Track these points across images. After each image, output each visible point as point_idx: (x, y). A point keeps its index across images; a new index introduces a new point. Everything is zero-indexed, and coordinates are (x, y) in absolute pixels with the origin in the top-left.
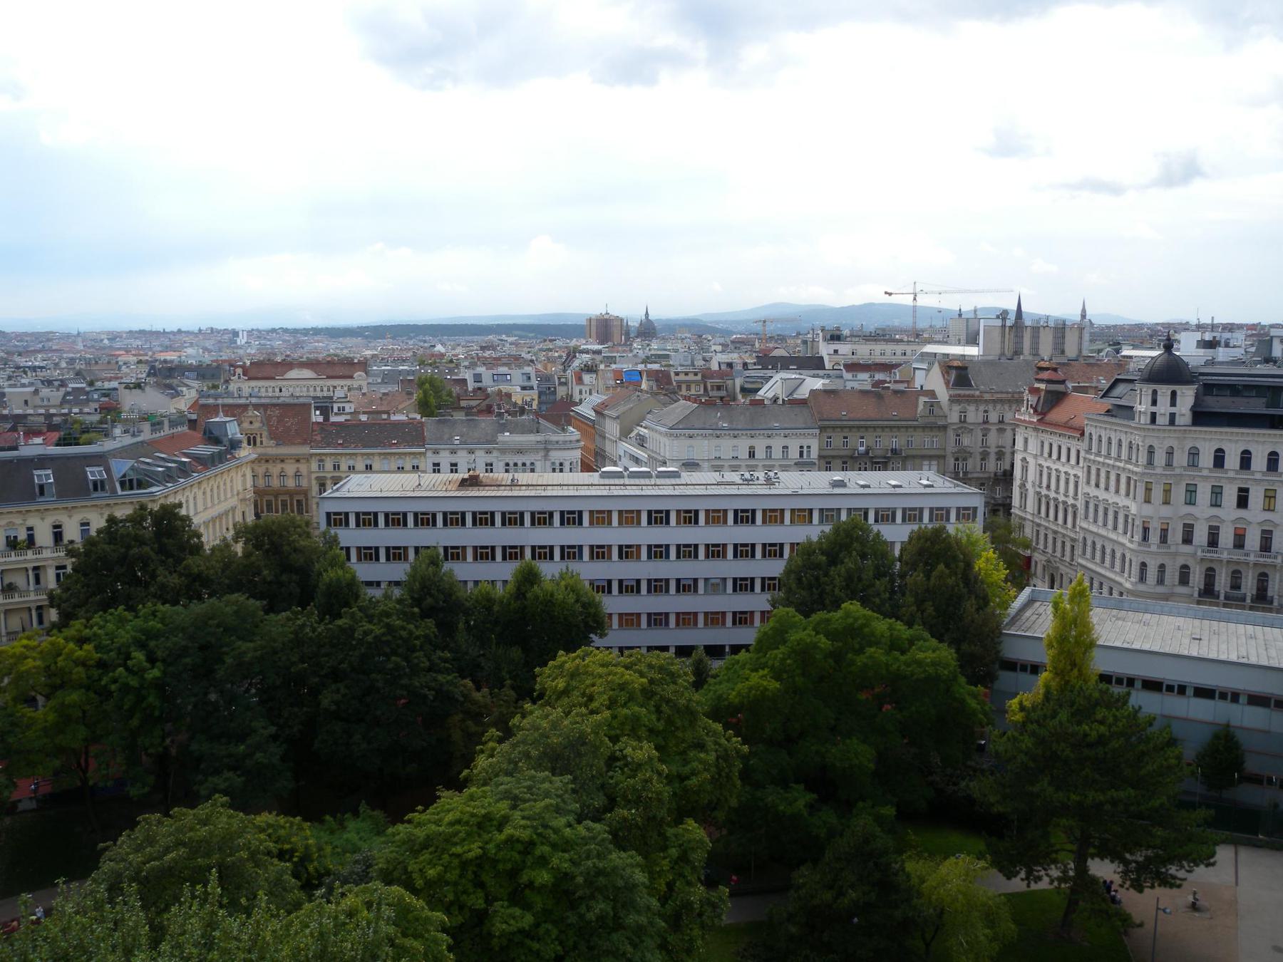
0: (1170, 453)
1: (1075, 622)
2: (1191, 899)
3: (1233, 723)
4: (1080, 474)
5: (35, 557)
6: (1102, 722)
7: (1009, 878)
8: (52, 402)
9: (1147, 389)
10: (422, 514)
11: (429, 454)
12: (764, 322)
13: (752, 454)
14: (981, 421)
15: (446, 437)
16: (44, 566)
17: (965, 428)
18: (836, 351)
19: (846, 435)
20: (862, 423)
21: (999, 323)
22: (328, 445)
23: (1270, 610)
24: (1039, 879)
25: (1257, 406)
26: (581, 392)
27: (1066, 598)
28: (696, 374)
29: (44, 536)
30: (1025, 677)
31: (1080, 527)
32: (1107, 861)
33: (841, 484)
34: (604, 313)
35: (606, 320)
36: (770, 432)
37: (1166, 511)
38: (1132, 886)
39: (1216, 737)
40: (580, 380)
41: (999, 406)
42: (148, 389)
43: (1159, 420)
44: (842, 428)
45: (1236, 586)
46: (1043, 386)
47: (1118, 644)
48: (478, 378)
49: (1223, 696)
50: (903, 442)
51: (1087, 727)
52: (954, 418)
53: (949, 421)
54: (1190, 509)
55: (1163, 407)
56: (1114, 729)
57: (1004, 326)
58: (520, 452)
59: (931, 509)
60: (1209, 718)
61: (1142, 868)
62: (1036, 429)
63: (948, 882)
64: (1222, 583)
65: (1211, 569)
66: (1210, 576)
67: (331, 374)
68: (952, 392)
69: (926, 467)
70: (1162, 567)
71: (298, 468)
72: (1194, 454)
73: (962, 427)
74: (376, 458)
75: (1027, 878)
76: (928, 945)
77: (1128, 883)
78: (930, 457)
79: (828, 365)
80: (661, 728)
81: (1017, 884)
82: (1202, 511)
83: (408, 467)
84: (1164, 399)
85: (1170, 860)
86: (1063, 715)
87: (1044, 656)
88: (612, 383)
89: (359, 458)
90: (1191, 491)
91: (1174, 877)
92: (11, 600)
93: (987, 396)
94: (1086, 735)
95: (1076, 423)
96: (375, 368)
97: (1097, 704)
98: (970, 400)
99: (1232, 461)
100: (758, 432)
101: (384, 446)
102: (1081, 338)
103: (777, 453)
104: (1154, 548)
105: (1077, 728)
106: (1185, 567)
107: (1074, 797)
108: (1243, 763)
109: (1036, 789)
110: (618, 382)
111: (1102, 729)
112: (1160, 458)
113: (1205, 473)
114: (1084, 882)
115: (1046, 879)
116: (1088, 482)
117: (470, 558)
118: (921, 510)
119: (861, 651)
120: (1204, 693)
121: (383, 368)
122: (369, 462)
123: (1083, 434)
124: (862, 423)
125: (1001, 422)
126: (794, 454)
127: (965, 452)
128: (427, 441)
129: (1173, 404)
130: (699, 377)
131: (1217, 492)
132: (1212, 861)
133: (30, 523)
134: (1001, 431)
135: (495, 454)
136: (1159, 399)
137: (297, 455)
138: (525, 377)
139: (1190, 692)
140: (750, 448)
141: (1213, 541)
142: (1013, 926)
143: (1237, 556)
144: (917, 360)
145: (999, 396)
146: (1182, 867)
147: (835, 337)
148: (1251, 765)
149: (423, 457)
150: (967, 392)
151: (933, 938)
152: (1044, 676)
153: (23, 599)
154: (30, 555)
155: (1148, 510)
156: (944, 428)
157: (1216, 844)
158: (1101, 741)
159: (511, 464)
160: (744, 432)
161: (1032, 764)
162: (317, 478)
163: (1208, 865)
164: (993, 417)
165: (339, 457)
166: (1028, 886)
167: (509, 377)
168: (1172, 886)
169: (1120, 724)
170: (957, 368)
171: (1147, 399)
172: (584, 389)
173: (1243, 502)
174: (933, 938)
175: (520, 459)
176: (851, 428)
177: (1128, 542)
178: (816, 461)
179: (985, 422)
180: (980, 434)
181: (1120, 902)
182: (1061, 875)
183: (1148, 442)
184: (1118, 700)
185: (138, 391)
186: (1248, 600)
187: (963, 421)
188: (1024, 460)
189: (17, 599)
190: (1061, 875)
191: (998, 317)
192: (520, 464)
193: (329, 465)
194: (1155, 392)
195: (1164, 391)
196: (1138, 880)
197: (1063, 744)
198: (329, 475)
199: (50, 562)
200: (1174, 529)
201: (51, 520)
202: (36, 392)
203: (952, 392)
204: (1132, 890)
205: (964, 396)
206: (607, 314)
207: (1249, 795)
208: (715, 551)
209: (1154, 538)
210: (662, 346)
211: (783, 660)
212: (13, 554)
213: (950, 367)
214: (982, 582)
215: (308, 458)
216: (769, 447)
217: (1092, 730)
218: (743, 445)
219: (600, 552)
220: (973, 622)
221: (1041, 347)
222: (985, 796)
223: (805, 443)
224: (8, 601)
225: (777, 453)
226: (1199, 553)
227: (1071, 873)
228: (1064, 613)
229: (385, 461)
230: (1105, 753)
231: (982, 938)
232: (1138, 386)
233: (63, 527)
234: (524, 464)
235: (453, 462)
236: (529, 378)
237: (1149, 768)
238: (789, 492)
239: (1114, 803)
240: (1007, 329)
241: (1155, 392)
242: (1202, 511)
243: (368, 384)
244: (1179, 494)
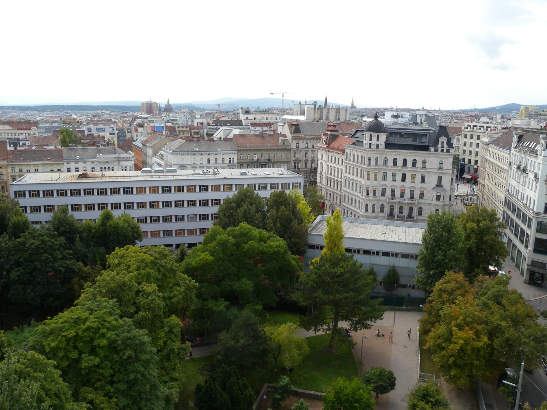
0: (377, 160)
1: (335, 228)
2: (377, 332)
3: (395, 265)
4: (343, 169)
6: (342, 267)
7: (308, 331)
9: (368, 134)
10: (60, 190)
11: (65, 164)
12: (219, 105)
13: (209, 162)
15: (73, 156)
17: (298, 150)
18: (247, 118)
19: (248, 153)
20: (256, 148)
21: (313, 106)
22: (16, 161)
23: (413, 221)
24: (319, 330)
25: (409, 141)
26: (137, 136)
27: (332, 218)
28: (187, 128)
30: (317, 251)
31: (343, 190)
32: (344, 321)
33: (245, 174)
36: (216, 152)
37: (375, 183)
38: (354, 330)
39: (390, 271)
40: (136, 131)
41: (312, 141)
43: (373, 147)
44: (247, 150)
45: (401, 212)
46: (329, 133)
47: (354, 236)
48: (89, 130)
49: (393, 255)
50: (273, 156)
51: (336, 270)
54: (384, 182)
55: (374, 142)
56: (346, 269)
57: (315, 108)
58: (107, 162)
59: (282, 184)
60: (388, 264)
61: (357, 322)
62: (326, 151)
63: (281, 334)
64: (396, 211)
65: (392, 206)
66: (392, 209)
67: (19, 128)
68: (292, 135)
69: (282, 166)
70: (374, 205)
72: (386, 160)
74: (40, 166)
75: (315, 330)
76: (276, 359)
77: (352, 328)
78: (284, 162)
79: (244, 124)
80: (160, 278)
81: (311, 333)
82: (389, 183)
83: (55, 170)
84: (374, 138)
85: (367, 319)
86: (327, 265)
87: (323, 242)
88: (150, 131)
89: (32, 166)
90: (385, 175)
91: (369, 325)
93: (307, 137)
94: (336, 273)
95: (341, 148)
96: (41, 125)
97: (340, 260)
98: (300, 138)
99: (400, 163)
100: (211, 152)
101: (44, 161)
102: (346, 113)
103: (220, 161)
104: (371, 198)
105: (332, 270)
106: (382, 205)
107: (331, 297)
108: (399, 280)
109: (316, 295)
111: (342, 270)
112: (373, 162)
113: (390, 168)
114: (336, 331)
115: (322, 330)
116: (346, 172)
117: (83, 209)
118: (278, 184)
119: (247, 243)
120: (386, 254)
121: (46, 125)
122: (36, 168)
123: (344, 152)
124: (256, 148)
125: (313, 147)
126: (227, 161)
128: (64, 158)
129: (378, 140)
130: (188, 129)
131: (394, 175)
132: (382, 317)
135: (96, 163)
136: (372, 138)
139: (381, 254)
141: (393, 195)
142: (308, 349)
143: (402, 200)
144: (280, 122)
145: (312, 137)
146: (372, 321)
147: (247, 112)
148: (402, 281)
150: (299, 135)
151: (278, 356)
152: (324, 250)
155: (368, 183)
156: (290, 150)
157: (384, 311)
158: (342, 274)
159: (103, 168)
160: (206, 152)
161: (315, 285)
162: (11, 176)
163: (380, 319)
164: (310, 146)
166: (315, 333)
168: (368, 328)
169: (349, 268)
170: (295, 125)
171: (368, 138)
172: (138, 134)
173: (404, 179)
174: (278, 356)
175: (107, 166)
176: (250, 150)
177: (361, 196)
178: (236, 164)
179: (307, 148)
181: (351, 336)
182: (327, 328)
183: (368, 155)
184: (348, 258)
186: (405, 218)
187: (297, 147)
188: (321, 163)
190: (327, 328)
191: (312, 104)
192: (107, 168)
193: (17, 170)
194: (371, 135)
195: (374, 135)
196: (356, 327)
197: (327, 277)
198: (17, 174)
200: (378, 191)
203: (292, 135)
204: (353, 331)
205: (298, 137)
206: (151, 101)
207: (402, 292)
208: (192, 203)
209: (371, 194)
210: (174, 115)
211: (214, 247)
214: (300, 213)
215: (6, 167)
216: (216, 159)
217: (338, 270)
218: (205, 158)
219: (141, 205)
220: (296, 229)
222: (298, 299)
223: (231, 157)
225: (220, 161)
226: (388, 200)
227: (331, 327)
228: (331, 224)
229: (45, 167)
230: (343, 279)
231: (295, 355)
232: (364, 133)
234: (109, 168)
235: (77, 167)
236: (113, 130)
237: (360, 284)
238: (222, 177)
239: (346, 298)
240: (316, 109)
241: (371, 135)
242: (389, 183)
243: (38, 132)
244: (380, 176)
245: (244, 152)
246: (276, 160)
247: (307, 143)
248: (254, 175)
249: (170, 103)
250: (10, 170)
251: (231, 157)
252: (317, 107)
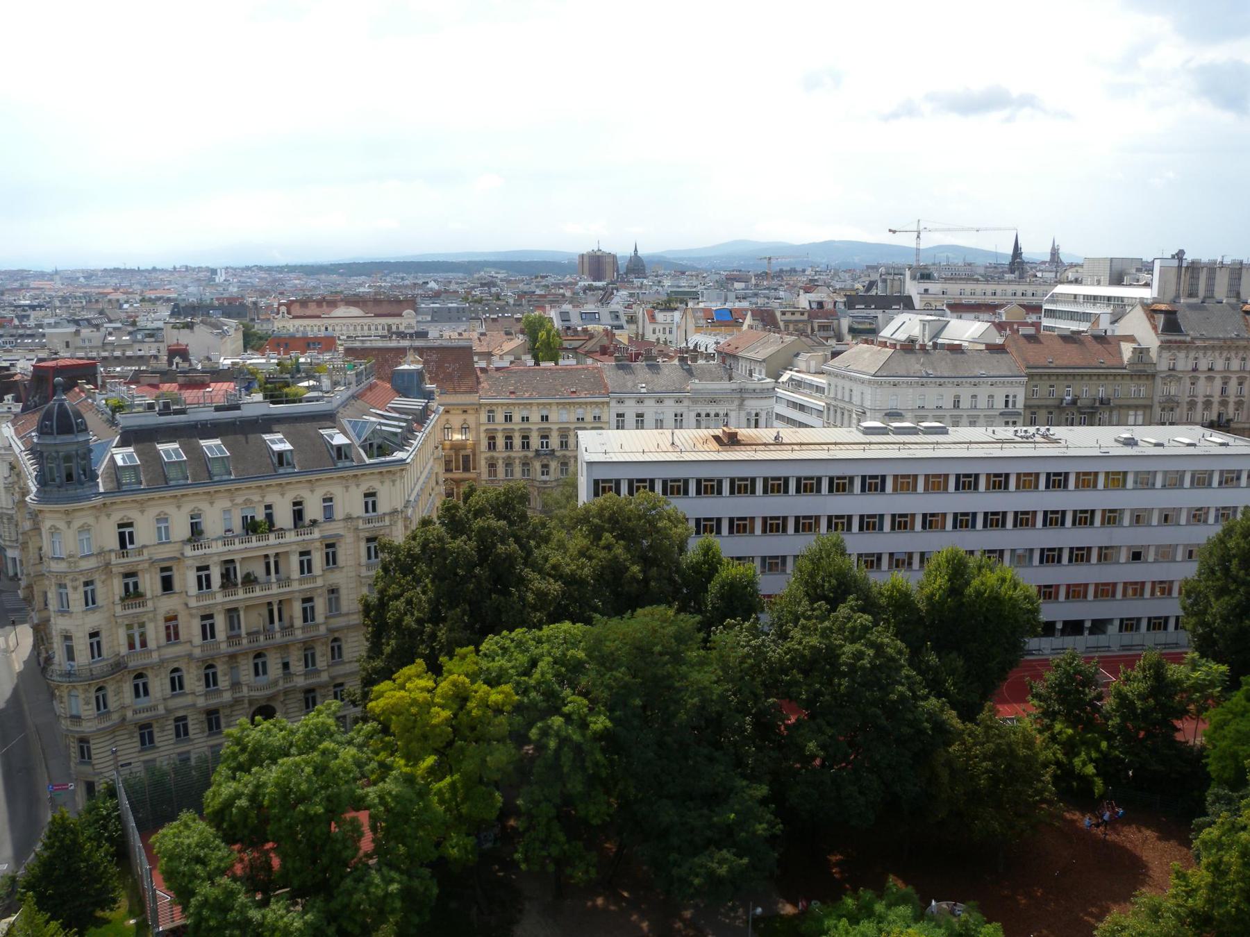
5: (278, 541)
8: (94, 343)
10: (706, 480)
11: (613, 403)
12: (770, 259)
13: (957, 404)
14: (1190, 368)
16: (287, 553)
17: (1175, 376)
18: (926, 291)
19: (1052, 383)
20: (1071, 371)
21: (1175, 263)
26: (654, 332)
28: (802, 314)
29: (283, 517)
33: (1130, 442)
34: (596, 249)
35: (598, 256)
36: (977, 380)
40: (653, 318)
41: (1209, 353)
42: (196, 328)
48: (565, 317)
50: (1110, 391)
52: (1163, 366)
53: (1158, 369)
57: (1180, 267)
58: (713, 401)
67: (378, 312)
71: (465, 420)
73: (1170, 376)
74: (554, 408)
78: (1136, 407)
79: (917, 303)
83: (589, 418)
88: (702, 322)
92: (252, 595)
93: (1198, 343)
98: (1180, 346)
103: (982, 403)
122: (545, 413)
124: (1071, 371)
126: (999, 404)
127: (1173, 401)
130: (805, 317)
133: (269, 500)
134: (1210, 379)
135: (686, 403)
140: (955, 397)
144: (1048, 302)
147: (926, 276)
150: (1178, 338)
153: (264, 593)
154: (272, 539)
156: (1153, 376)
159: (703, 415)
164: (1203, 365)
172: (658, 327)
178: (1022, 411)
179: (1195, 370)
180: (1188, 382)
185: (187, 331)
189: (258, 593)
191: (1173, 257)
192: (712, 414)
193: (500, 417)
198: (500, 427)
199: (294, 547)
201: (291, 496)
202: (77, 333)
205: (1176, 342)
206: (599, 250)
208: (1024, 519)
210: (676, 283)
212: (254, 538)
213: (1155, 311)
215: (478, 408)
216: (974, 397)
219: (870, 523)
221: (1216, 289)
223: (1011, 391)
224: (248, 595)
225: (982, 403)
229: (564, 412)
233: (305, 504)
236: (617, 317)
238: (1097, 453)
243: (418, 322)
245: (1041, 379)
246: (1118, 402)
247: (1196, 358)
248: (1157, 445)
249: (639, 253)
250: (483, 417)
251: (1011, 391)
252: (1185, 265)
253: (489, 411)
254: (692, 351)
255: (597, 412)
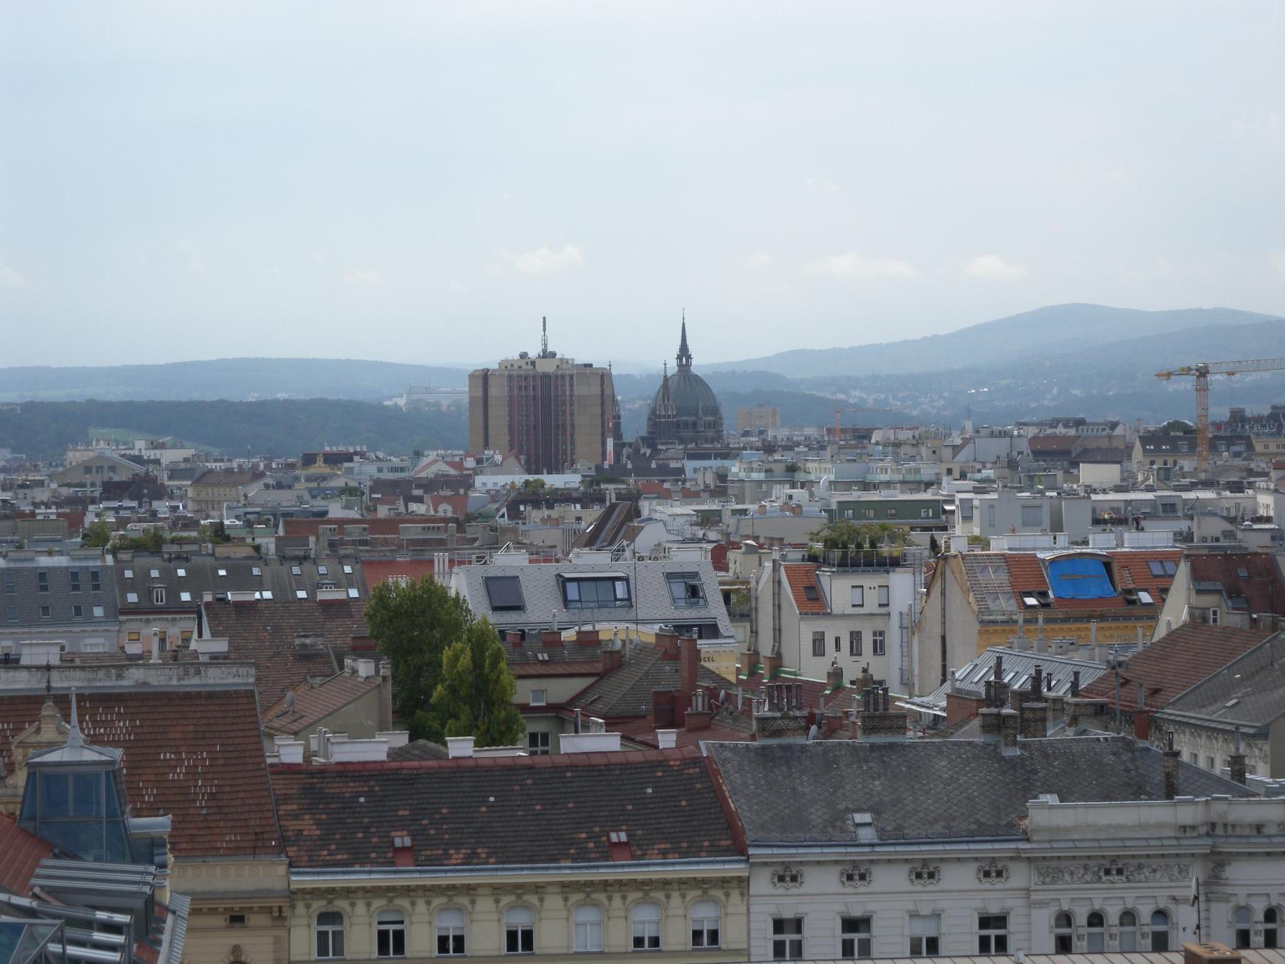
11: (762, 883)
12: (1203, 373)
15: (817, 814)
22: (357, 857)
34: (534, 351)
35: (545, 376)
40: (813, 599)
74: (554, 902)
88: (1005, 605)
89: (485, 904)
101: (582, 856)
110: (1145, 597)
122: (520, 920)
128: (750, 836)
135: (1019, 876)
137: (236, 895)
138: (679, 589)
149: (735, 896)
159: (1081, 917)
165: (404, 903)
167: (620, 589)
172: (832, 630)
192: (1113, 914)
206: (547, 355)
210: (853, 471)
229: (588, 915)
234: (1128, 917)
235: (857, 912)
236: (694, 592)
249: (701, 361)
253: (325, 918)
254: (1022, 696)
255: (705, 915)
